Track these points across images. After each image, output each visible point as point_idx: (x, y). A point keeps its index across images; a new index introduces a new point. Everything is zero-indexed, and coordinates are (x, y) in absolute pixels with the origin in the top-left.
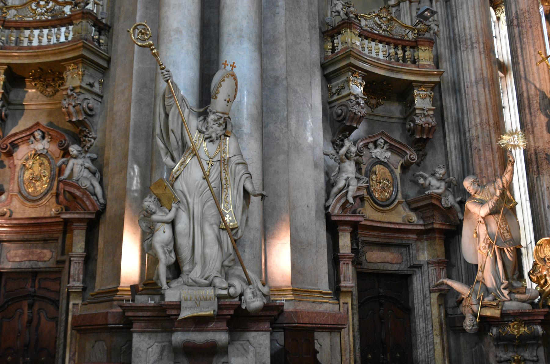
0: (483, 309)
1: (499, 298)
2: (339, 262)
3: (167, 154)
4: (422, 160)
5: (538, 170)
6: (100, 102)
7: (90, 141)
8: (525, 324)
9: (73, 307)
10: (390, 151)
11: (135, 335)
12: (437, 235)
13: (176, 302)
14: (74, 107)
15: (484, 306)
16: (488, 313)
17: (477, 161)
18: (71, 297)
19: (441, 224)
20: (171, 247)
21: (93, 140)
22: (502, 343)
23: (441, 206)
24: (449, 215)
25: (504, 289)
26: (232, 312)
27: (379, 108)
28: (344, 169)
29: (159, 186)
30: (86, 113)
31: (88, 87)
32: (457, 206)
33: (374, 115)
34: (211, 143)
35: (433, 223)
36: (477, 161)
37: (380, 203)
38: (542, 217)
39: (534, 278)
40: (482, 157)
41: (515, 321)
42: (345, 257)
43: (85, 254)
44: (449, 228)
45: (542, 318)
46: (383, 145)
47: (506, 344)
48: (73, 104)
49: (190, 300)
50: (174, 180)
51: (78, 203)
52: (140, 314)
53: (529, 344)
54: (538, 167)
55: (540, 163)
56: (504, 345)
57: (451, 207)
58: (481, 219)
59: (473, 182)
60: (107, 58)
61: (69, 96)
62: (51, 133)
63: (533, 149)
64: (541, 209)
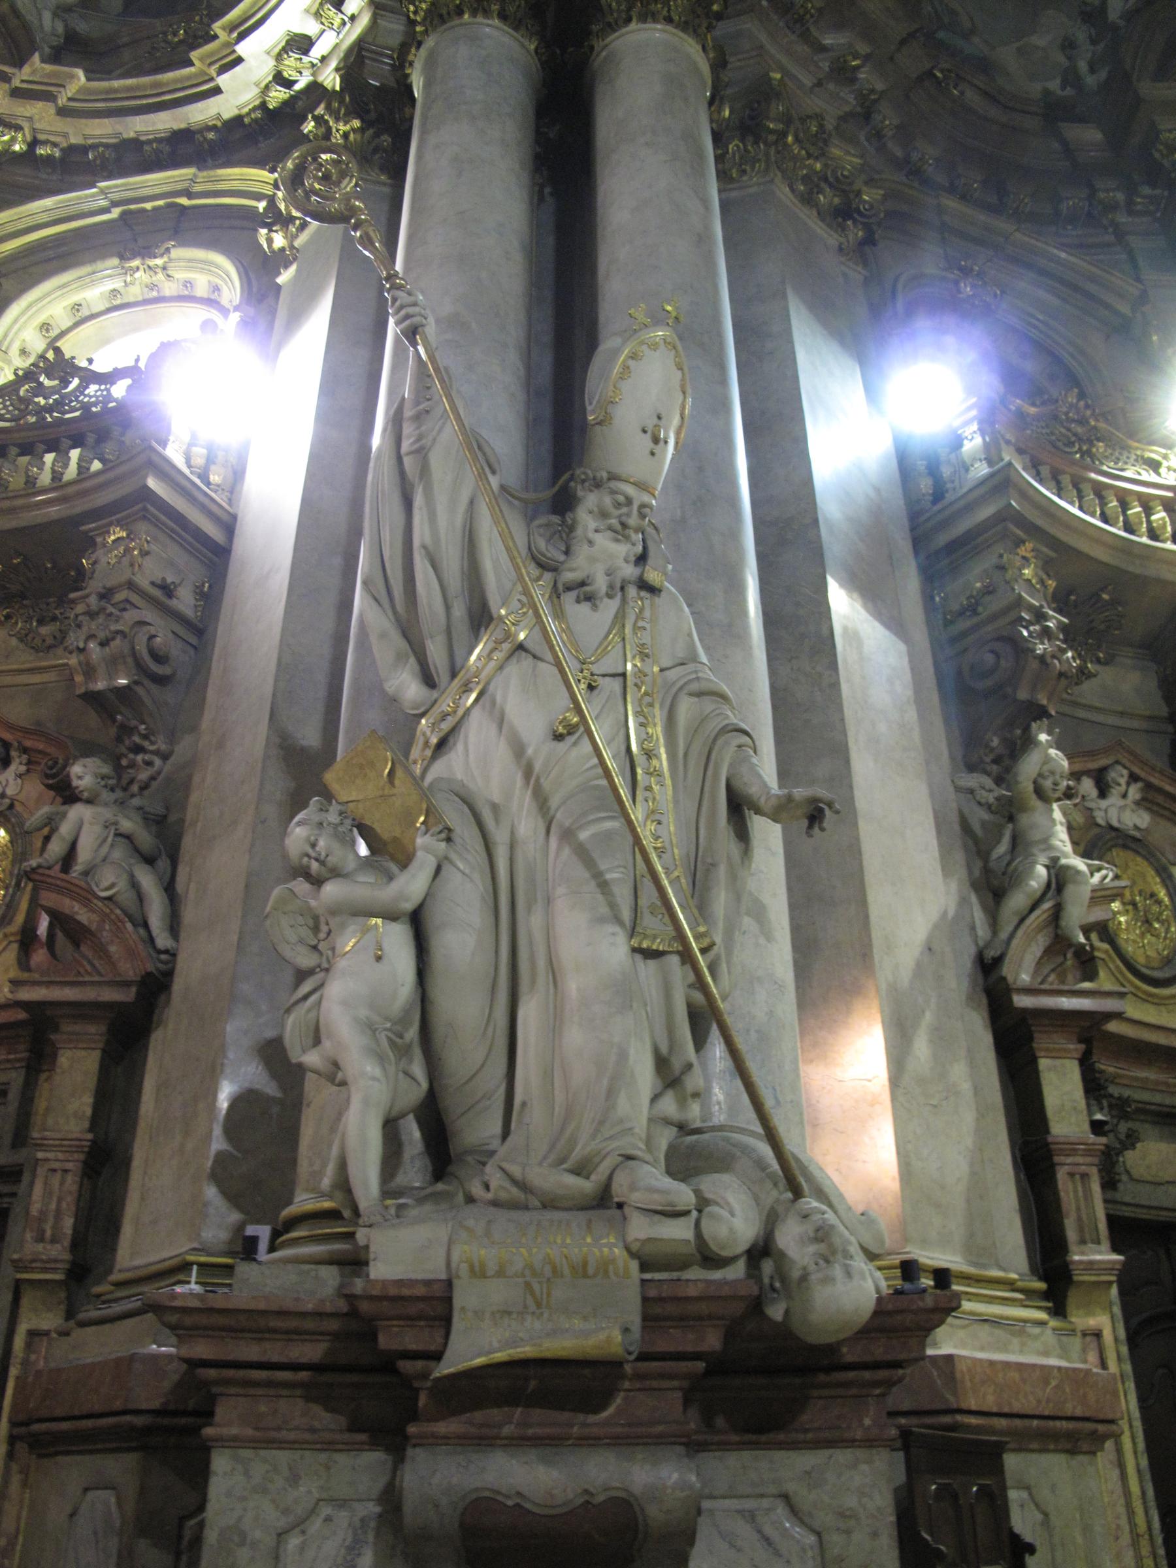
2: (1051, 1169)
3: (400, 658)
6: (195, 648)
7: (149, 764)
9: (29, 1346)
10: (1148, 809)
11: (220, 1462)
13: (428, 1283)
14: (102, 644)
18: (25, 1302)
20: (412, 1033)
21: (158, 762)
26: (713, 1341)
27: (1087, 686)
28: (1036, 835)
29: (361, 767)
30: (139, 666)
31: (157, 593)
33: (1075, 704)
34: (585, 607)
37: (1144, 970)
42: (1071, 1148)
43: (90, 1136)
46: (1124, 787)
48: (102, 635)
49: (501, 1273)
50: (429, 753)
51: (84, 957)
52: (250, 1351)
60: (225, 517)
61: (92, 615)
62: (28, 743)
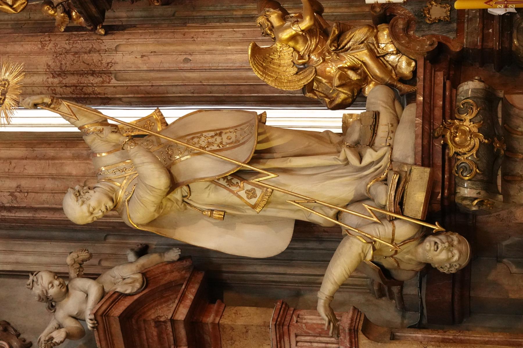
0: (407, 212)
1: (383, 172)
4: (18, 335)
5: (101, 73)
8: (453, 118)
12: (210, 319)
15: (400, 205)
16: (417, 198)
17: (44, 197)
19: (180, 302)
22: (499, 182)
23: (136, 297)
24: (163, 282)
25: (361, 158)
32: (144, 260)
35: (173, 321)
36: (44, 197)
38: (208, 79)
39: (342, 96)
40: (37, 184)
41: (444, 136)
44: (197, 286)
45: (440, 77)
47: (503, 175)
53: (504, 121)
54: (93, 73)
55: (83, 67)
56: (503, 180)
57: (144, 274)
58: (177, 195)
59: (78, 195)
63: (51, 80)
64: (189, 79)
